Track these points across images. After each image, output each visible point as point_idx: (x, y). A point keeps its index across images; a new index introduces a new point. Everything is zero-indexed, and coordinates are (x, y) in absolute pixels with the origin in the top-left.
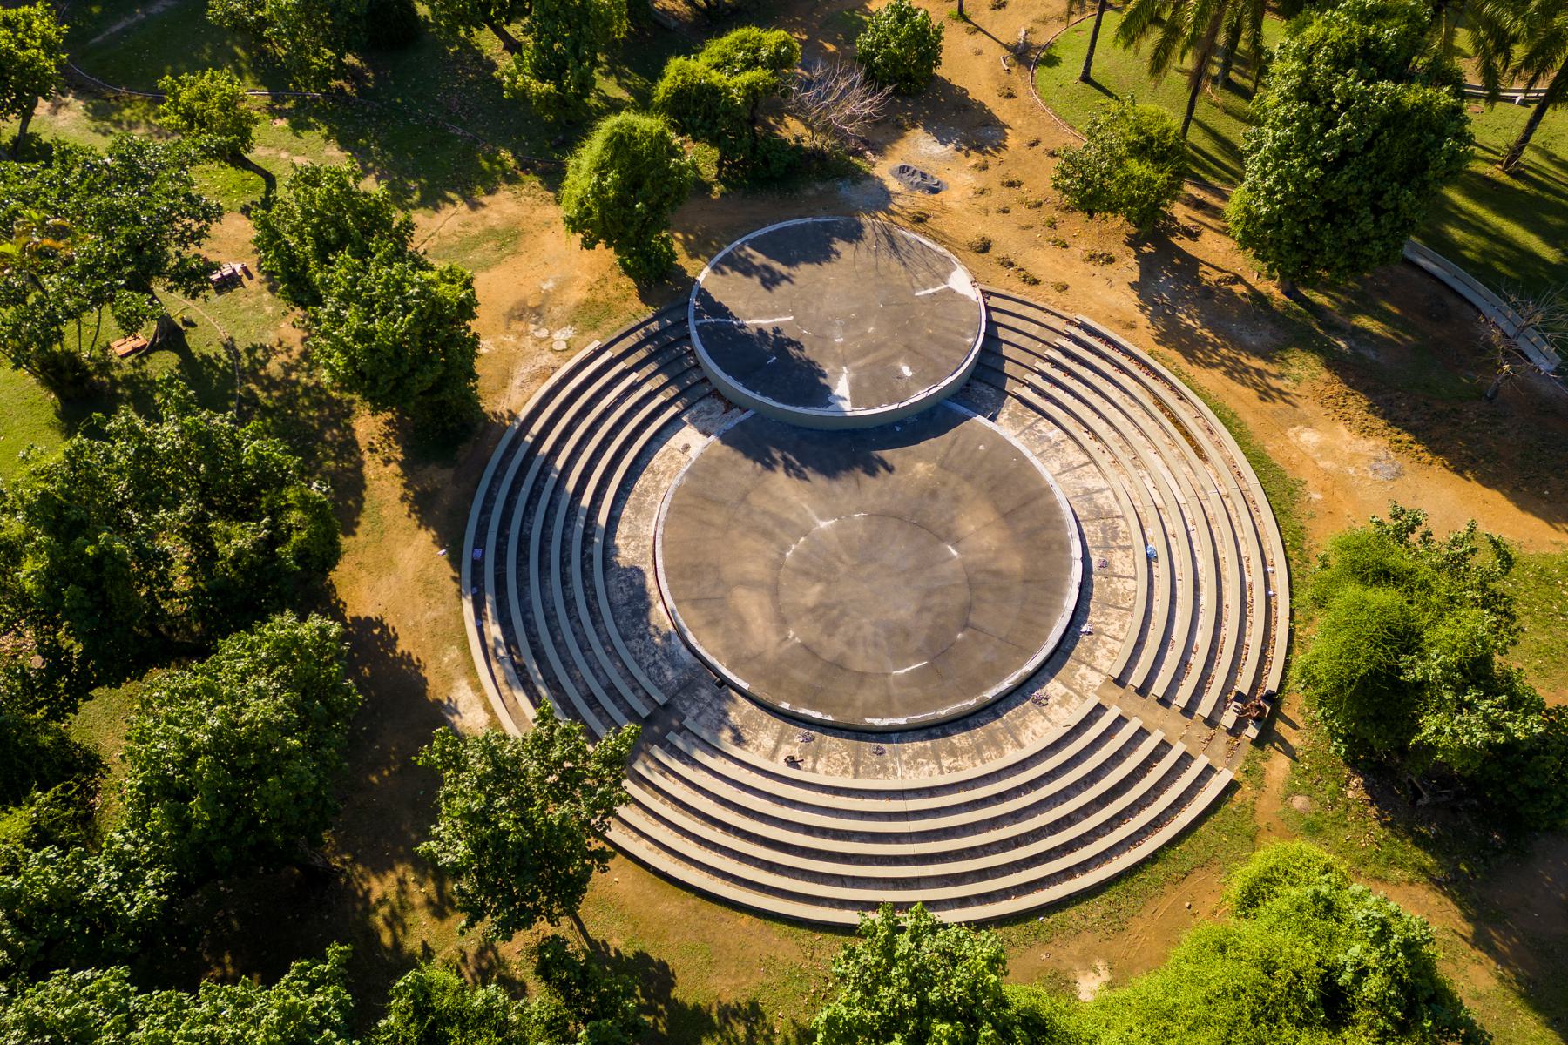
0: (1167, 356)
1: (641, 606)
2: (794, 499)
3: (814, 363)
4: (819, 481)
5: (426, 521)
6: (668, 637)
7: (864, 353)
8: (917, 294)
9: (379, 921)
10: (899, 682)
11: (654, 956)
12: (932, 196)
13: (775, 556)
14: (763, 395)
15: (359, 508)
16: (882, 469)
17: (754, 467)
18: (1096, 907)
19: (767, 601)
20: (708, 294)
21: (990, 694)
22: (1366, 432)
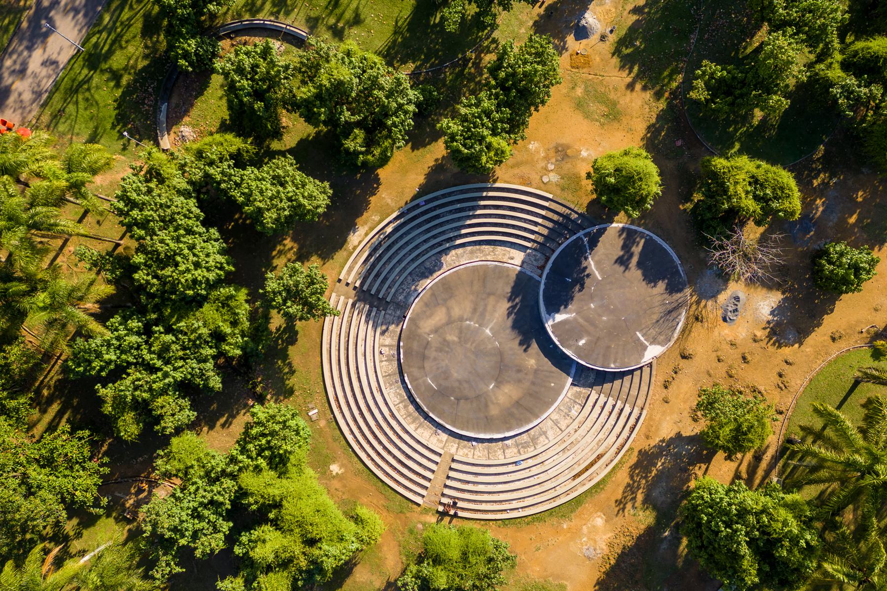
0: (632, 456)
1: (427, 274)
2: (497, 315)
3: (572, 300)
4: (510, 322)
5: (428, 176)
6: (416, 290)
7: (587, 320)
8: (638, 333)
9: (278, 248)
10: (425, 382)
11: (298, 336)
12: (721, 319)
13: (465, 317)
14: (545, 284)
15: (424, 146)
16: (524, 347)
17: (508, 293)
18: (361, 466)
19: (444, 321)
20: (603, 233)
21: (431, 415)
22: (610, 545)
